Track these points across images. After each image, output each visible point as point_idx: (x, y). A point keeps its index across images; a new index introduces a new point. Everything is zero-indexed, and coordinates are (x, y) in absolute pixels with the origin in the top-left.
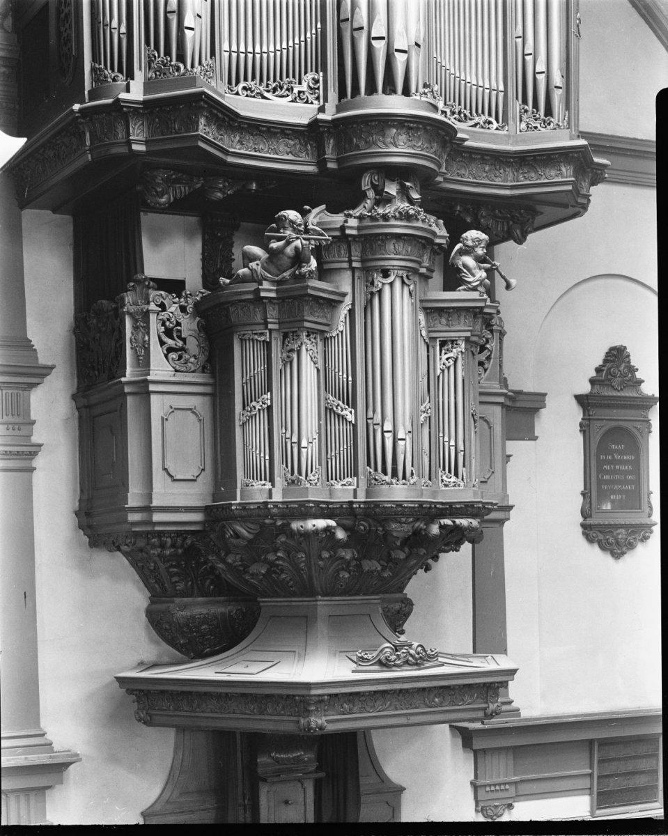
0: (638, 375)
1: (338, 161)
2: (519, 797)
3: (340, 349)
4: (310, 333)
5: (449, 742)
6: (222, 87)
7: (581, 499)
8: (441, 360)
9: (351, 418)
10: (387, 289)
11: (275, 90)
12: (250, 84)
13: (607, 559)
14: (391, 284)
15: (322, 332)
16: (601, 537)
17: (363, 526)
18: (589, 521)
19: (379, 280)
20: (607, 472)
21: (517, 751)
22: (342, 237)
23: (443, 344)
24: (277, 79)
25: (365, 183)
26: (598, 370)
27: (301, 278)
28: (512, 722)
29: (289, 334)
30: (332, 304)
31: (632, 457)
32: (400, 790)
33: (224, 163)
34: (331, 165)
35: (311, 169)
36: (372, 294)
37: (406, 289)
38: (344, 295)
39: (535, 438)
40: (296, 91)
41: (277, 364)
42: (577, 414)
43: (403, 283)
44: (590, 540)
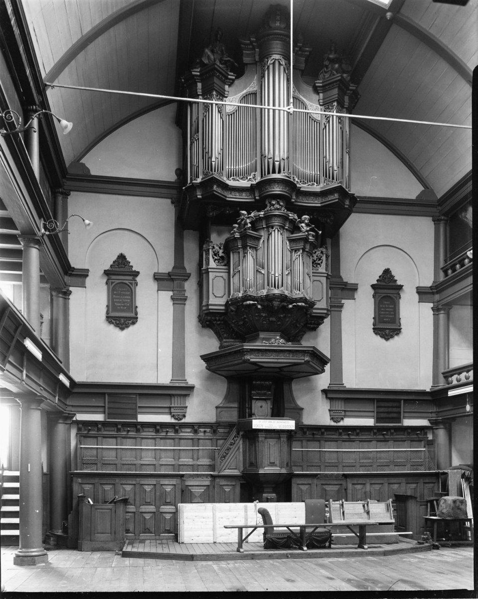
0: (395, 278)
1: (259, 196)
2: (345, 416)
3: (260, 252)
4: (251, 247)
5: (321, 397)
6: (225, 179)
7: (373, 320)
8: (295, 256)
9: (263, 272)
10: (273, 232)
11: (242, 178)
12: (235, 177)
13: (383, 341)
14: (274, 231)
15: (255, 248)
16: (380, 332)
17: (266, 303)
18: (375, 327)
19: (271, 230)
20: (382, 311)
21: (346, 400)
22: (259, 219)
23: (295, 251)
24: (243, 175)
25: (267, 202)
26: (380, 277)
27: (246, 229)
28: (343, 389)
29: (245, 247)
30: (258, 239)
31: (393, 306)
32: (302, 409)
33: (226, 200)
34: (257, 198)
35: (253, 200)
36: (269, 235)
37: (279, 233)
38: (262, 236)
39: (355, 299)
40: (249, 178)
41: (241, 258)
42: (372, 292)
43: (278, 231)
44: (376, 334)
